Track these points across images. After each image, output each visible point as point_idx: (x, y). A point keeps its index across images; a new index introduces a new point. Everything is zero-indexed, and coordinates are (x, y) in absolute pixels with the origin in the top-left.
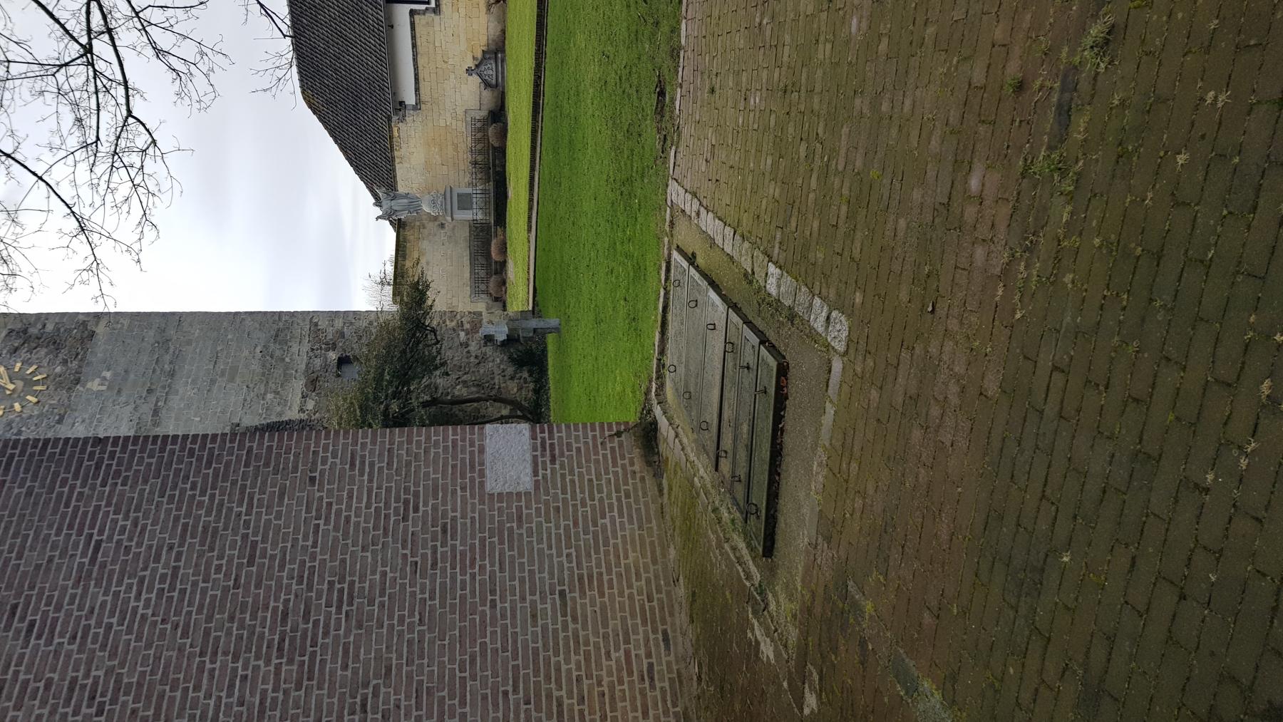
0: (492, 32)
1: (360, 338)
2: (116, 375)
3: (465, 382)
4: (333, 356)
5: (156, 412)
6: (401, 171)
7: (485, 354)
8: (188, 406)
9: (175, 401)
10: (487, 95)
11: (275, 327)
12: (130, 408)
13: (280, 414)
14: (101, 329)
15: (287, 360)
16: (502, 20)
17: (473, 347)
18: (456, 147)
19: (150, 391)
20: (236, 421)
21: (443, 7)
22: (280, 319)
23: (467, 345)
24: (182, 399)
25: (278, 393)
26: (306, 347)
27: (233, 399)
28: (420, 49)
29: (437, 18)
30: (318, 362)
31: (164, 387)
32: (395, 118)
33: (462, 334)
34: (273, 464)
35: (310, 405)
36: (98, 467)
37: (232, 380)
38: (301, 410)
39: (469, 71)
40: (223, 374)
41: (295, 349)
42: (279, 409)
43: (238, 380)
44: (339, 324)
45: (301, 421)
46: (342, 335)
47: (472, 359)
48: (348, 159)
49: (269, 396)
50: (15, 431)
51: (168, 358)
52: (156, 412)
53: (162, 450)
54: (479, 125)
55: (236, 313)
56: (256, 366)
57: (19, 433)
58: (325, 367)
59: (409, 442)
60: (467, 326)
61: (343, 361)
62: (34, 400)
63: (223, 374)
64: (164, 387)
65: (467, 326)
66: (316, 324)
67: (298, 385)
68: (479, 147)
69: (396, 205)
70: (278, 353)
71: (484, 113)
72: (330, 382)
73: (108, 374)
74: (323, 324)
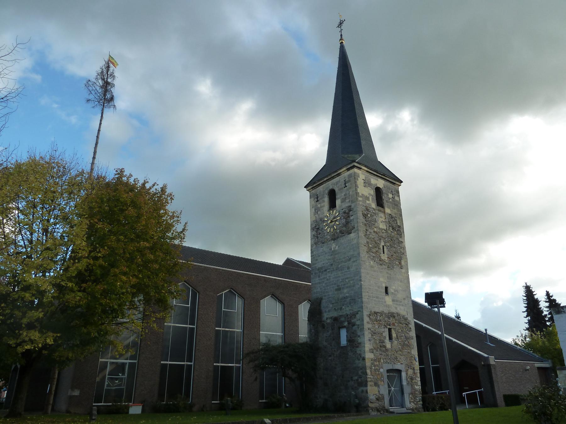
1: (353, 333)
8: (327, 280)
13: (326, 312)
14: (352, 235)
15: (343, 307)
23: (352, 380)
26: (348, 313)
27: (330, 293)
30: (343, 319)
33: (356, 378)
35: (328, 321)
40: (338, 286)
41: (347, 309)
44: (358, 323)
46: (354, 325)
49: (331, 306)
52: (326, 270)
65: (360, 380)
66: (357, 314)
67: (335, 314)
74: (358, 316)
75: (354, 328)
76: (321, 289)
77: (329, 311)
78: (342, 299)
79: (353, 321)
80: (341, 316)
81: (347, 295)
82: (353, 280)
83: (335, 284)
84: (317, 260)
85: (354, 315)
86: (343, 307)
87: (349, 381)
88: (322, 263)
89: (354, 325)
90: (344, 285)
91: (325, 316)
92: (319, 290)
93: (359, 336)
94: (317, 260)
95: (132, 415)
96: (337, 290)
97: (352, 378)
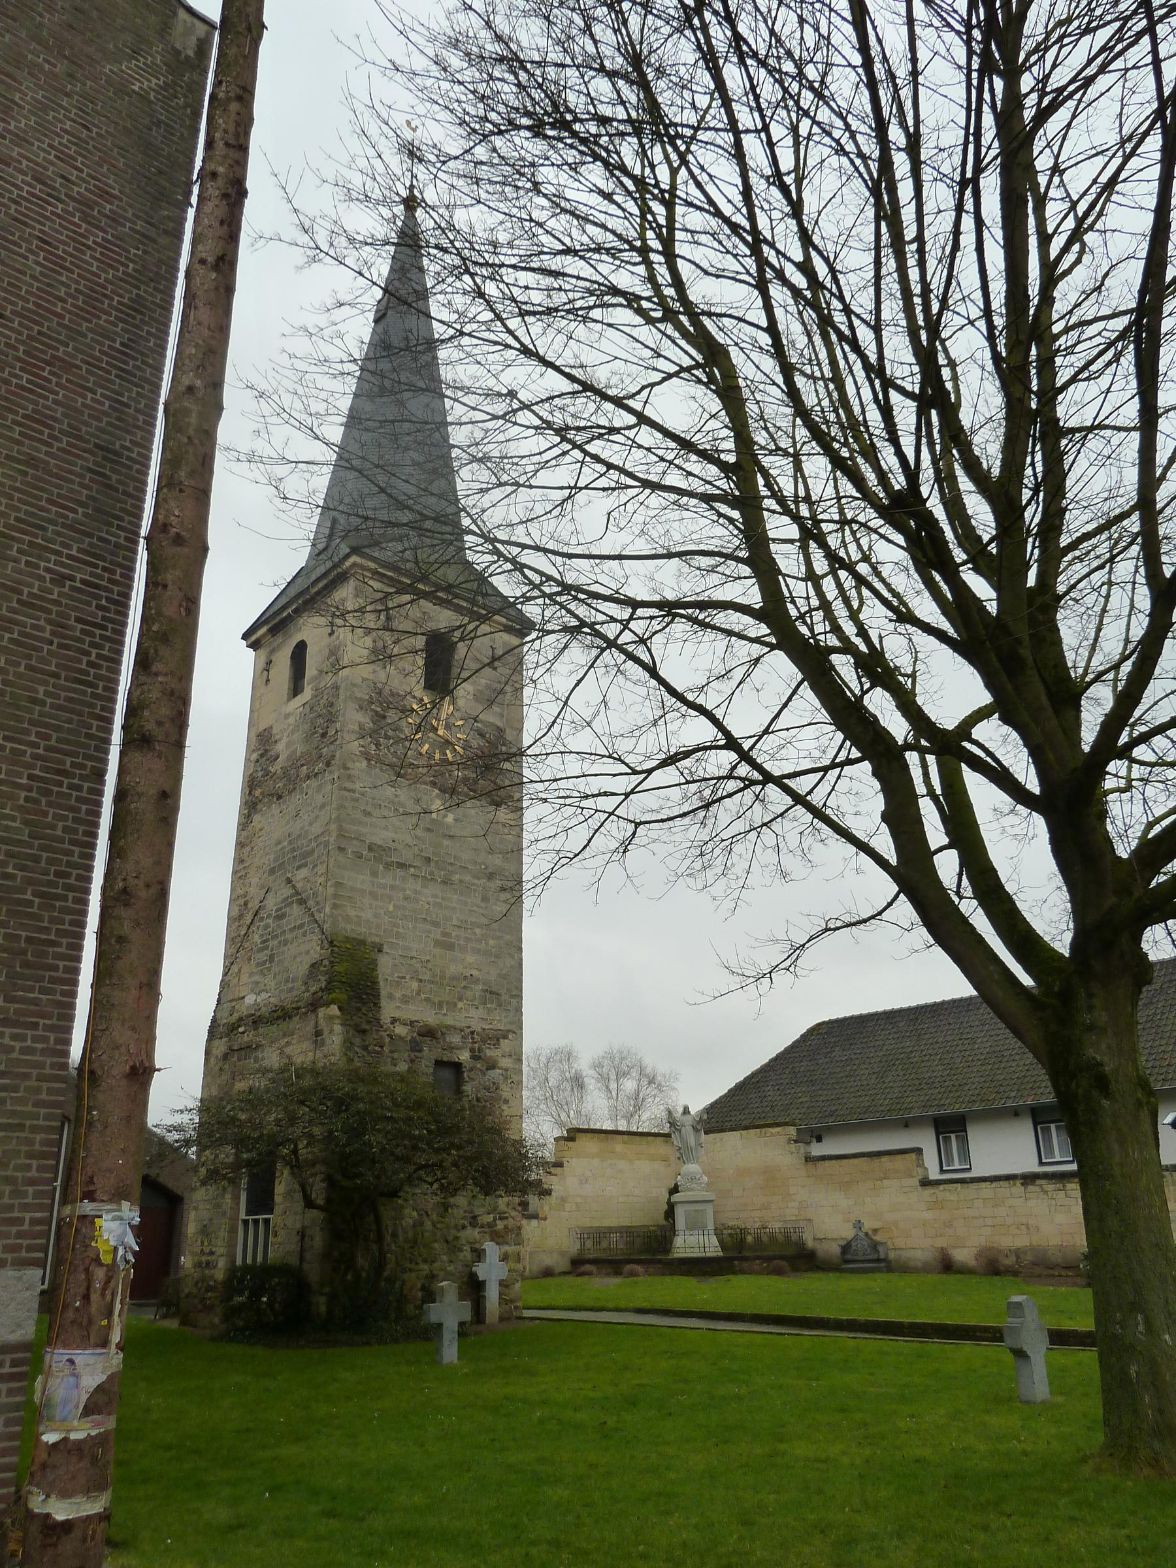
0: (910, 1254)
1: (488, 1089)
2: (449, 827)
3: (422, 1224)
4: (464, 1056)
5: (401, 865)
6: (732, 1139)
7: (460, 1250)
8: (406, 898)
9: (411, 886)
10: (835, 1249)
11: (503, 992)
12: (409, 841)
13: (391, 997)
14: (503, 815)
15: (460, 1005)
16: (925, 1269)
17: (472, 1233)
18: (765, 1207)
19: (428, 860)
20: (386, 949)
21: (929, 1191)
22: (512, 996)
24: (416, 892)
25: (418, 994)
26: (477, 1026)
27: (414, 945)
28: (876, 1161)
29: (915, 1182)
30: (455, 1039)
31: (431, 874)
32: (792, 1131)
34: (26, 971)
35: (401, 1030)
36: (59, 772)
37: (437, 943)
38: (394, 1021)
39: (858, 1225)
40: (444, 934)
41: (473, 1013)
42: (398, 995)
43: (437, 951)
44: (505, 1063)
45: (378, 1020)
46: (492, 1066)
47: (453, 1232)
48: (753, 1075)
49: (415, 985)
50: (390, 733)
51: (468, 878)
52: (401, 865)
53: (73, 842)
54: (794, 1237)
55: (520, 949)
56: (453, 969)
57: (387, 737)
58: (452, 1048)
59: (30, 1155)
60: (500, 1225)
61: (457, 1067)
62: (424, 751)
63: (444, 934)
64: (431, 874)
65: (500, 1225)
66: (505, 1037)
67: (429, 1017)
68: (765, 1239)
69: (688, 1131)
70: (469, 994)
71: (810, 1244)
72: (430, 1054)
73: (450, 818)
74: (504, 1043)
75: (494, 1074)
76: (376, 916)
77: (405, 1000)
78: (454, 978)
79: (489, 1053)
80: (449, 1027)
81: (475, 973)
82: (499, 938)
83: (436, 924)
84: (367, 814)
85: (496, 1038)
86: (460, 1005)
87: (464, 1227)
88: (391, 835)
89: (492, 1066)
90: (467, 940)
91: (388, 1010)
92: (367, 915)
93: (506, 1102)
94: (367, 814)
95: (1098, 1322)
96: (437, 943)
97: (475, 1217)
